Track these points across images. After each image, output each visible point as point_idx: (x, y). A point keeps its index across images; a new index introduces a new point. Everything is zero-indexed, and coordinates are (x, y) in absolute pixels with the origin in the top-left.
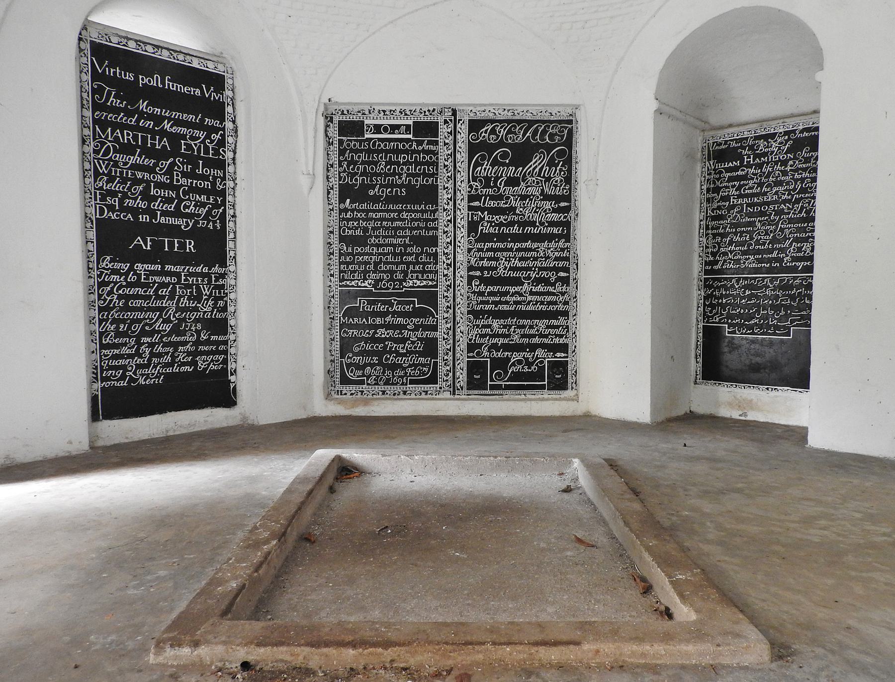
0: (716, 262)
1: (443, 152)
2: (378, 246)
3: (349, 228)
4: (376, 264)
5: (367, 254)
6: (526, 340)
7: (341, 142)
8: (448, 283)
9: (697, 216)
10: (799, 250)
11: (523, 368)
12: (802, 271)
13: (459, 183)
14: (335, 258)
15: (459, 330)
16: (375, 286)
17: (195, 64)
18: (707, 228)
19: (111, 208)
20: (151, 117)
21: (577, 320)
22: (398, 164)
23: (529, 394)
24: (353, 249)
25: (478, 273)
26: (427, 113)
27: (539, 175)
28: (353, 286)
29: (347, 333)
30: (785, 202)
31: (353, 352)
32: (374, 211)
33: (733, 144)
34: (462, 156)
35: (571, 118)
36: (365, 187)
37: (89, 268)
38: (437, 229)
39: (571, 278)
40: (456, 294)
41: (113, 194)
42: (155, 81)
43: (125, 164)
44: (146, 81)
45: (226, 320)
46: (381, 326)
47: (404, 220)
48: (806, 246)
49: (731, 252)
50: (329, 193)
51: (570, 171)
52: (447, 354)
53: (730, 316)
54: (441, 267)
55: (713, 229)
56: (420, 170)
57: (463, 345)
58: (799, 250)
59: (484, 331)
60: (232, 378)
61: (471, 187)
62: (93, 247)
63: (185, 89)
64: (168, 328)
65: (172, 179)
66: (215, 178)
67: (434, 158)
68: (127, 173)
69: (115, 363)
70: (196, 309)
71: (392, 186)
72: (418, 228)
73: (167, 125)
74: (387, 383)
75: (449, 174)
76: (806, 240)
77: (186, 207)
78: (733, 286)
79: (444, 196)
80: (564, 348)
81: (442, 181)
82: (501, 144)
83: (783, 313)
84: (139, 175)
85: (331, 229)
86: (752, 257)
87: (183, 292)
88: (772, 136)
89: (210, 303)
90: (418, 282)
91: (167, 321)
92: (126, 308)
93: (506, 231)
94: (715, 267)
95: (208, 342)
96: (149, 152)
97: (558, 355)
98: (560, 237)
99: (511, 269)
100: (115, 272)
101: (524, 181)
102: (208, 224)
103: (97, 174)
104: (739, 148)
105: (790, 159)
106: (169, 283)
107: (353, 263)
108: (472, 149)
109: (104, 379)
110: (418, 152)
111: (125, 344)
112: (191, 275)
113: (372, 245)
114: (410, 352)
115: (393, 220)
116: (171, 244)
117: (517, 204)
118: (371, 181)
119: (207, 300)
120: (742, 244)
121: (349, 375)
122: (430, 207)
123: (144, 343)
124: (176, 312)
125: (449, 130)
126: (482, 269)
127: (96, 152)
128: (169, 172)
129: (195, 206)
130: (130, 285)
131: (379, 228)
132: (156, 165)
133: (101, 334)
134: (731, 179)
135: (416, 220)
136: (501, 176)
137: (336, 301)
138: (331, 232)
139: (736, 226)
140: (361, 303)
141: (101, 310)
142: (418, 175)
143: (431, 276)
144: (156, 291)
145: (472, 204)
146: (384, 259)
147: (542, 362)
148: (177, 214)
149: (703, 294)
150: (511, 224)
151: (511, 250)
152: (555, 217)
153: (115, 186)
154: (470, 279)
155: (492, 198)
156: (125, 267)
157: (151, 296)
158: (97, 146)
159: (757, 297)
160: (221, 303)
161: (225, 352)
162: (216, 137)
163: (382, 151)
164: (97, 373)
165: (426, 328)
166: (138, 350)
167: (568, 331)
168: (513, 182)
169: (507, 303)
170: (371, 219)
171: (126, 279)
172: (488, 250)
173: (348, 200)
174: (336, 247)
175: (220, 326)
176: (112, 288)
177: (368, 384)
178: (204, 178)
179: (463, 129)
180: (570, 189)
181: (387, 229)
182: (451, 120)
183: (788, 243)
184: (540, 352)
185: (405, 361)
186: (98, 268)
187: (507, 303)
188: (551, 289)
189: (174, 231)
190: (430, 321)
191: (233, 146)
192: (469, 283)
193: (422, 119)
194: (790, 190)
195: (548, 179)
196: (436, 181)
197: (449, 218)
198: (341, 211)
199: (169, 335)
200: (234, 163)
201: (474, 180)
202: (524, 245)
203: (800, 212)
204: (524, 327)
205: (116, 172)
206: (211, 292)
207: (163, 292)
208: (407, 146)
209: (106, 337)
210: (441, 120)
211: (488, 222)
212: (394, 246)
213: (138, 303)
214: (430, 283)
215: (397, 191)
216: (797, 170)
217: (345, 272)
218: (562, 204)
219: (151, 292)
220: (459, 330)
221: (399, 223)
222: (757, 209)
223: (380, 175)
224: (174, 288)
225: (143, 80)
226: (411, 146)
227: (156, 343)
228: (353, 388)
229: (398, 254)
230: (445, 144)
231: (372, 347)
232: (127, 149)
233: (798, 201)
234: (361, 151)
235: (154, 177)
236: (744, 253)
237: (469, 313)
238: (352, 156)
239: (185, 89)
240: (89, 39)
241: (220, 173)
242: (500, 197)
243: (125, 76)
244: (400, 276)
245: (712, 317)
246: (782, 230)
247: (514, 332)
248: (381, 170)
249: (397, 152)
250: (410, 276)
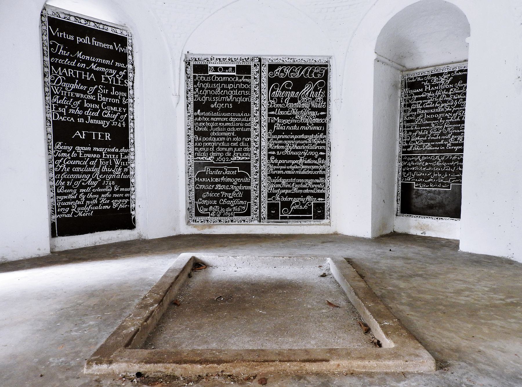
0: (409, 147)
1: (254, 83)
2: (216, 137)
3: (200, 127)
4: (215, 147)
5: (210, 142)
6: (301, 191)
7: (195, 77)
8: (257, 158)
9: (398, 120)
10: (456, 139)
12: (457, 152)
13: (263, 101)
14: (192, 144)
15: (263, 185)
16: (214, 160)
17: (110, 31)
18: (404, 127)
19: (61, 114)
20: (84, 61)
21: (330, 180)
22: (228, 89)
23: (303, 222)
24: (202, 139)
25: (274, 153)
26: (244, 60)
27: (309, 97)
28: (202, 160)
29: (199, 187)
30: (448, 112)
31: (202, 198)
32: (214, 117)
33: (419, 79)
34: (265, 85)
35: (327, 64)
36: (209, 103)
37: (49, 149)
38: (250, 127)
39: (327, 155)
40: (261, 165)
41: (62, 106)
42: (86, 40)
43: (69, 88)
44: (81, 40)
45: (129, 179)
46: (218, 183)
47: (231, 122)
48: (460, 138)
49: (417, 141)
50: (188, 106)
51: (326, 94)
52: (256, 199)
53: (416, 177)
54: (252, 149)
55: (407, 127)
56: (240, 93)
57: (265, 194)
58: (456, 139)
59: (277, 186)
60: (133, 213)
61: (269, 103)
62: (51, 137)
63: (104, 45)
64: (95, 184)
65: (97, 97)
66: (122, 97)
67: (248, 86)
68: (70, 94)
69: (65, 204)
70: (111, 173)
71: (224, 102)
72: (239, 127)
73: (93, 66)
74: (222, 215)
75: (257, 96)
76: (459, 134)
77: (105, 114)
78: (418, 160)
79: (254, 108)
80: (323, 195)
81: (253, 99)
82: (287, 78)
83: (446, 175)
84: (78, 95)
85: (189, 127)
86: (429, 144)
87: (104, 163)
88: (441, 74)
89: (120, 169)
90: (240, 158)
91: (95, 180)
92: (71, 172)
93: (290, 129)
94: (408, 150)
95: (118, 192)
96: (83, 82)
97: (319, 199)
98: (320, 132)
99: (293, 150)
100: (64, 151)
101: (300, 100)
102: (118, 124)
103: (53, 94)
104: (422, 81)
105: (451, 88)
106: (96, 158)
107: (202, 147)
108: (271, 81)
109: (58, 213)
110: (239, 83)
111: (71, 193)
112: (109, 153)
113: (213, 136)
114: (235, 198)
115: (225, 122)
116: (97, 136)
118: (212, 99)
119: (118, 168)
120: (423, 136)
121: (200, 211)
122: (246, 115)
123: (81, 193)
124: (100, 175)
125: (257, 70)
126: (276, 150)
127: (52, 81)
128: (95, 93)
129: (110, 113)
130: (73, 159)
131: (217, 127)
132: (87, 89)
133: (56, 187)
134: (418, 99)
135: (238, 122)
136: (287, 97)
137: (192, 169)
138: (189, 129)
139: (420, 126)
140: (207, 170)
141: (56, 173)
142: (239, 96)
143: (247, 154)
144: (88, 162)
145: (270, 113)
146: (220, 145)
147: (310, 204)
148: (100, 118)
149: (401, 164)
150: (293, 124)
151: (292, 139)
152: (318, 120)
153: (63, 101)
154: (269, 156)
155: (282, 109)
156: (70, 148)
157: (85, 165)
158: (53, 78)
159: (432, 167)
160: (126, 170)
161: (129, 198)
162: (122, 73)
163: (218, 82)
164: (55, 210)
165: (244, 184)
166: (78, 196)
167: (325, 186)
168: (293, 100)
169: (290, 170)
170: (212, 122)
171: (70, 156)
172: (279, 139)
173: (199, 110)
174: (192, 137)
175: (125, 182)
176: (63, 161)
177: (211, 216)
178: (116, 97)
179: (265, 69)
180: (326, 105)
181: (222, 127)
182: (258, 65)
183: (449, 135)
184: (309, 198)
185: (232, 203)
186: (54, 149)
187: (290, 170)
188: (315, 162)
189: (98, 128)
190: (246, 180)
191: (132, 78)
192: (269, 159)
193: (241, 63)
194: (451, 105)
195: (314, 99)
196: (250, 100)
197: (257, 121)
198: (195, 117)
199: (96, 187)
200: (133, 89)
201: (272, 99)
202: (300, 137)
203: (457, 118)
204: (300, 183)
205: (64, 93)
206: (120, 163)
207: (92, 163)
208: (233, 79)
209: (60, 189)
210: (252, 64)
211: (279, 123)
212: (226, 137)
213: (78, 169)
214: (246, 158)
215: (227, 105)
216: (455, 94)
217: (197, 152)
218: (322, 113)
219: (85, 163)
220: (263, 185)
221: (228, 124)
222: (432, 116)
223: (217, 96)
224: (99, 161)
225: (79, 40)
226: (235, 79)
227: (88, 193)
228: (202, 218)
229: (228, 142)
230: (255, 78)
231: (213, 195)
232: (70, 80)
233: (455, 112)
234: (206, 82)
235: (86, 97)
236: (425, 141)
237: (268, 175)
238: (201, 85)
239: (104, 45)
240: (47, 15)
241: (125, 95)
242: (286, 109)
243: (69, 37)
244: (229, 154)
245: (406, 178)
246: (446, 128)
247: (294, 186)
248: (217, 94)
249: (227, 83)
250: (235, 154)
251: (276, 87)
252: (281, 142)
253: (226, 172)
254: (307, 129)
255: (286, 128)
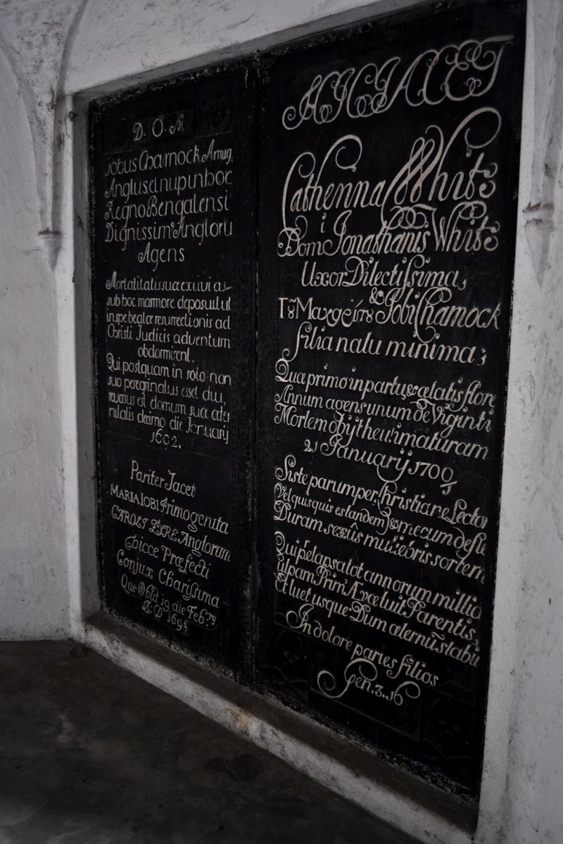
2: (149, 361)
3: (117, 328)
4: (150, 395)
6: (379, 624)
11: (373, 687)
27: (424, 200)
56: (204, 205)
72: (201, 331)
82: (344, 125)
101: (387, 218)
110: (200, 168)
114: (189, 577)
117: (374, 279)
150: (358, 331)
151: (355, 395)
155: (325, 264)
169: (346, 522)
172: (315, 391)
181: (161, 329)
187: (346, 522)
195: (445, 208)
204: (377, 590)
211: (314, 323)
221: (176, 320)
223: (148, 222)
247: (358, 595)
251: (305, 171)
252: (314, 400)
253: (172, 485)
254: (413, 353)
255: (334, 345)
